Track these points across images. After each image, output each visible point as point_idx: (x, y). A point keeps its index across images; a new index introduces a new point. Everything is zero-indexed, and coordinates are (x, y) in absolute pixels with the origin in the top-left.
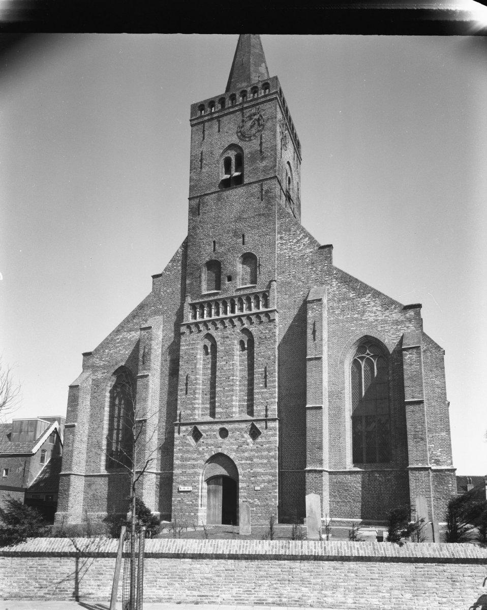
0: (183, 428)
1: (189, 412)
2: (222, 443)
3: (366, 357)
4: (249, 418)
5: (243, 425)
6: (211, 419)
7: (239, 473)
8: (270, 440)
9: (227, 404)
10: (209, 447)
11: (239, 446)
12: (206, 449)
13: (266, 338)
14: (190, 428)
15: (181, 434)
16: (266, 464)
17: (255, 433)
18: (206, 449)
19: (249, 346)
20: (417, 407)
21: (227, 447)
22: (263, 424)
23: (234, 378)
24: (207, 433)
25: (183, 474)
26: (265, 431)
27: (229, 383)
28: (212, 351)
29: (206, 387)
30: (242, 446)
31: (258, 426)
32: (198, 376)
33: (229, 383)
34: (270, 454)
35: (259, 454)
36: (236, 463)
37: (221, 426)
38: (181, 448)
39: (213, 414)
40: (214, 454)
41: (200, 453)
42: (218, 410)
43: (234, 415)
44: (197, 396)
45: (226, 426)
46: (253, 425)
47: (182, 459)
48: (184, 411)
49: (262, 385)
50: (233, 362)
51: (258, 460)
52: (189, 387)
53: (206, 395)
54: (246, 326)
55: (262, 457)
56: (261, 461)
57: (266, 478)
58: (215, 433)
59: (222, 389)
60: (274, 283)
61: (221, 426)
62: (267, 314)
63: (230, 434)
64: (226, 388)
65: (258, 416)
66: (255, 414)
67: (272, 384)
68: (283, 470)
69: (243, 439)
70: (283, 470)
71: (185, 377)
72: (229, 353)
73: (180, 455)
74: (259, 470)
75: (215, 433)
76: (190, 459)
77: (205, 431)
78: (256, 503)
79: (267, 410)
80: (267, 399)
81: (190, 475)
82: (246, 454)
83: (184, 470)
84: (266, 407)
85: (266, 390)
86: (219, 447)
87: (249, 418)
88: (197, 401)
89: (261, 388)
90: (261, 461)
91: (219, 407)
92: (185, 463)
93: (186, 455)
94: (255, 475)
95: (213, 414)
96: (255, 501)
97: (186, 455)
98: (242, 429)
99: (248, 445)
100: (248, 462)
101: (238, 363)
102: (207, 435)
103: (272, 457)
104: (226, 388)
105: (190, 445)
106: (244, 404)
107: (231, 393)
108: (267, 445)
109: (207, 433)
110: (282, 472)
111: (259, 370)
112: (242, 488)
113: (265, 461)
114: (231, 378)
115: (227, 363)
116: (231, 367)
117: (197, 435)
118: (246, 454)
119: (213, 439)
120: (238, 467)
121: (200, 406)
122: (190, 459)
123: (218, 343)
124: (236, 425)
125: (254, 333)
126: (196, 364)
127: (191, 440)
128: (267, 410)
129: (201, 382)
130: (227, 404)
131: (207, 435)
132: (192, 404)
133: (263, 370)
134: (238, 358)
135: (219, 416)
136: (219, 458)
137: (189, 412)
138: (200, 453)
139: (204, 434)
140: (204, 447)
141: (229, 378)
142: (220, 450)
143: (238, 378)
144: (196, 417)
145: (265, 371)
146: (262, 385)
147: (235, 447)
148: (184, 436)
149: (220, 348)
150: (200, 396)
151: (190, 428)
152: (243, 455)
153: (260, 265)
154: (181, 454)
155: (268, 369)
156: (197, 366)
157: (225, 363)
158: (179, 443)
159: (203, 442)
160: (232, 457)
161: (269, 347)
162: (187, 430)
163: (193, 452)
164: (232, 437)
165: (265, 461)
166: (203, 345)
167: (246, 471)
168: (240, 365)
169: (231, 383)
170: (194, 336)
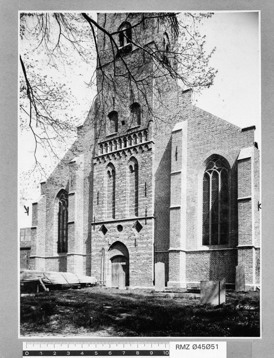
0: (96, 226)
1: (100, 216)
2: (119, 235)
3: (213, 170)
6: (113, 220)
7: (129, 254)
8: (148, 232)
9: (122, 209)
11: (129, 237)
13: (146, 162)
14: (100, 226)
16: (146, 247)
17: (139, 227)
19: (135, 170)
20: (246, 204)
21: (122, 237)
22: (144, 221)
23: (126, 191)
24: (110, 229)
26: (145, 226)
27: (123, 195)
28: (113, 174)
29: (109, 199)
30: (131, 237)
32: (104, 192)
33: (123, 195)
34: (148, 241)
35: (142, 241)
36: (127, 247)
37: (118, 224)
38: (95, 239)
39: (114, 217)
40: (114, 242)
42: (116, 213)
43: (126, 216)
44: (104, 205)
45: (121, 224)
46: (137, 222)
49: (143, 195)
50: (126, 181)
51: (141, 245)
52: (99, 199)
53: (110, 204)
54: (133, 155)
56: (142, 246)
58: (115, 229)
59: (119, 199)
60: (151, 122)
61: (118, 224)
62: (146, 145)
64: (121, 199)
66: (139, 215)
67: (150, 194)
68: (157, 251)
69: (132, 232)
70: (157, 251)
71: (97, 193)
72: (123, 175)
74: (142, 252)
75: (115, 229)
77: (109, 228)
78: (139, 273)
79: (146, 212)
80: (147, 204)
84: (146, 209)
86: (117, 238)
88: (104, 208)
89: (143, 197)
90: (142, 246)
91: (117, 211)
94: (138, 255)
98: (131, 225)
99: (134, 235)
101: (129, 181)
102: (110, 230)
104: (121, 199)
105: (101, 237)
106: (132, 208)
107: (124, 202)
108: (146, 235)
109: (110, 229)
110: (156, 252)
113: (145, 246)
114: (124, 192)
115: (121, 181)
116: (124, 184)
117: (104, 230)
119: (114, 233)
120: (129, 250)
121: (106, 212)
123: (116, 169)
125: (138, 159)
126: (103, 184)
127: (101, 233)
128: (146, 212)
129: (106, 196)
130: (122, 209)
131: (110, 230)
132: (101, 210)
133: (144, 184)
134: (129, 177)
136: (118, 245)
137: (100, 216)
139: (109, 230)
141: (123, 192)
142: (118, 240)
143: (128, 192)
144: (104, 219)
145: (146, 185)
146: (143, 195)
147: (127, 237)
149: (117, 172)
150: (106, 205)
153: (142, 111)
154: (95, 243)
155: (147, 183)
156: (104, 186)
157: (120, 182)
160: (125, 244)
161: (148, 168)
162: (98, 227)
165: (145, 246)
166: (107, 171)
167: (134, 252)
168: (130, 183)
169: (124, 195)
170: (101, 165)
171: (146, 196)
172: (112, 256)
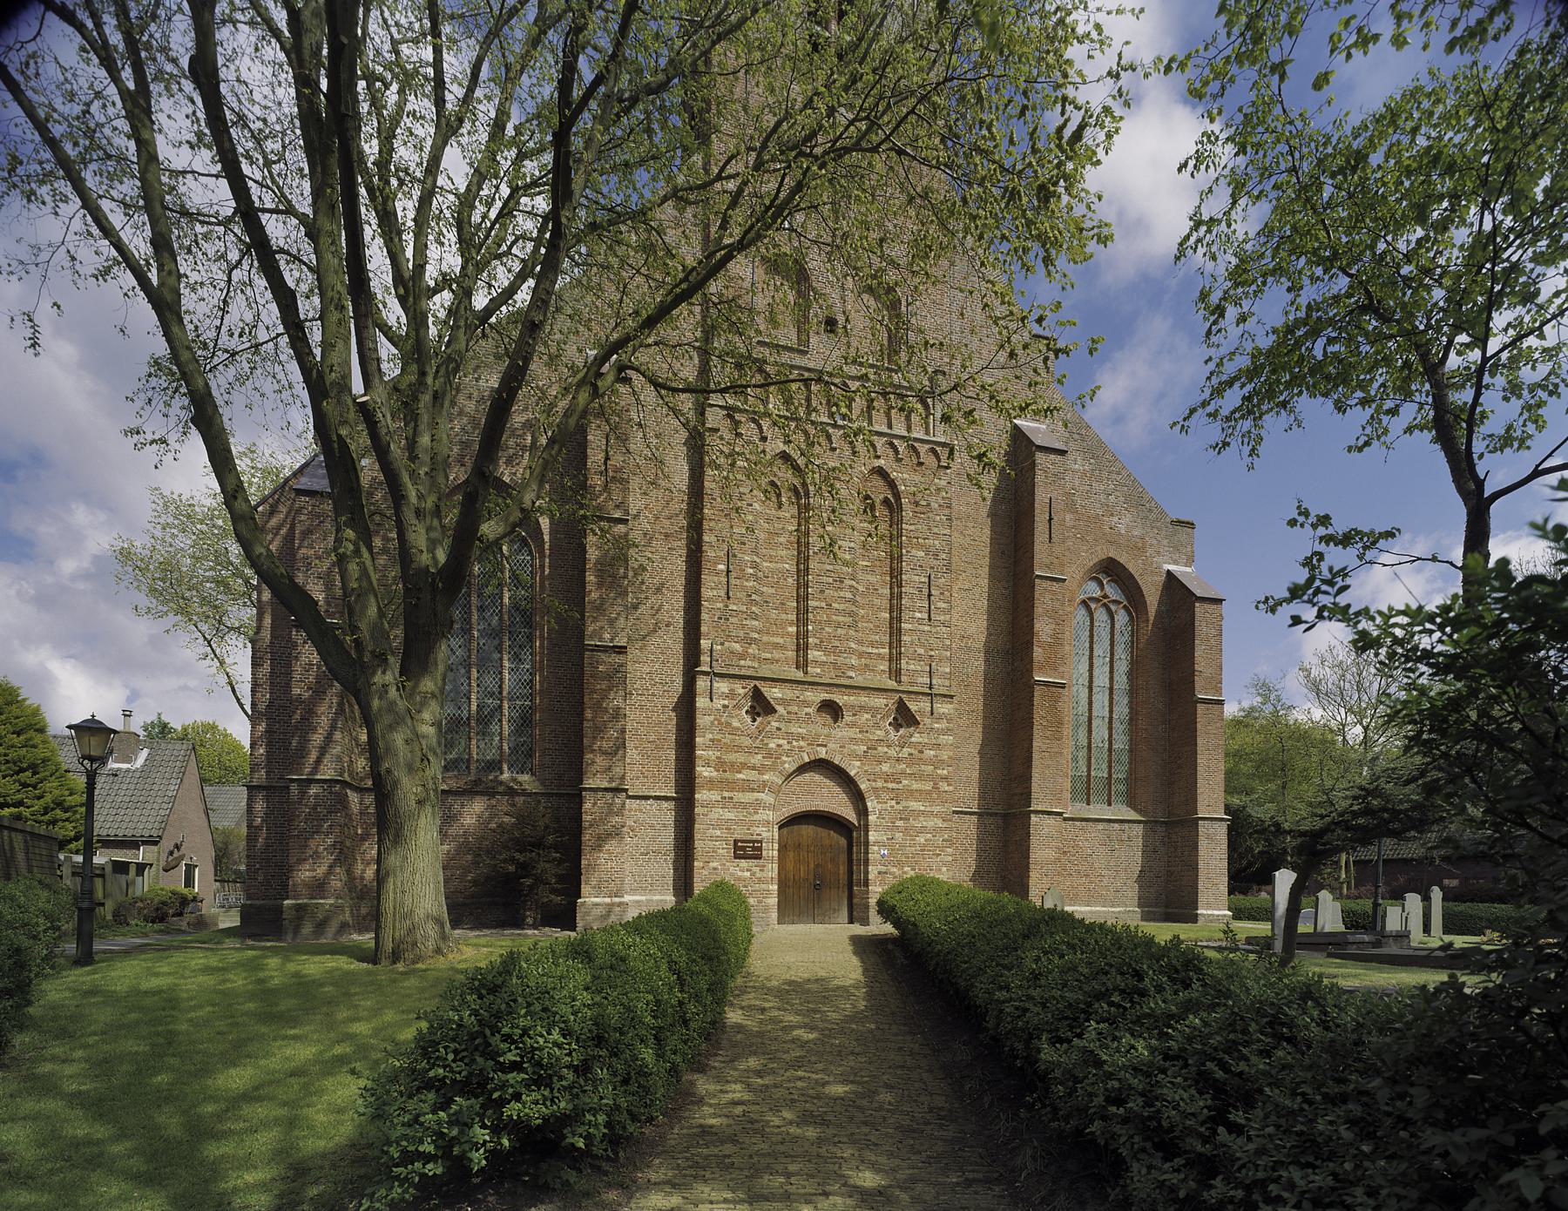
0: (722, 686)
4: (892, 684)
5: (879, 701)
6: (799, 675)
8: (939, 741)
10: (795, 743)
12: (787, 747)
15: (719, 703)
16: (929, 793)
18: (787, 747)
21: (838, 743)
24: (790, 709)
25: (726, 802)
26: (928, 721)
27: (842, 594)
31: (913, 707)
35: (915, 769)
39: (802, 664)
41: (769, 755)
42: (813, 654)
45: (840, 699)
46: (901, 703)
47: (720, 765)
48: (722, 644)
52: (733, 581)
55: (920, 777)
57: (930, 823)
61: (827, 696)
63: (848, 718)
65: (911, 684)
66: (904, 678)
73: (712, 754)
74: (915, 805)
76: (744, 766)
77: (783, 702)
81: (744, 806)
82: (885, 768)
83: (726, 794)
85: (927, 628)
87: (892, 684)
91: (818, 647)
92: (727, 775)
93: (731, 757)
95: (802, 664)
96: (905, 873)
97: (731, 757)
100: (890, 785)
103: (944, 778)
109: (790, 709)
111: (913, 579)
112: (876, 843)
113: (928, 786)
117: (761, 706)
118: (885, 768)
120: (866, 795)
122: (744, 766)
124: (863, 699)
127: (741, 719)
135: (819, 670)
138: (769, 755)
140: (781, 742)
142: (822, 753)
148: (725, 706)
151: (740, 689)
152: (878, 769)
158: (712, 723)
159: (779, 729)
162: (732, 694)
163: (750, 751)
164: (852, 725)
165: (928, 786)
171: (930, 620)
172: (786, 812)
